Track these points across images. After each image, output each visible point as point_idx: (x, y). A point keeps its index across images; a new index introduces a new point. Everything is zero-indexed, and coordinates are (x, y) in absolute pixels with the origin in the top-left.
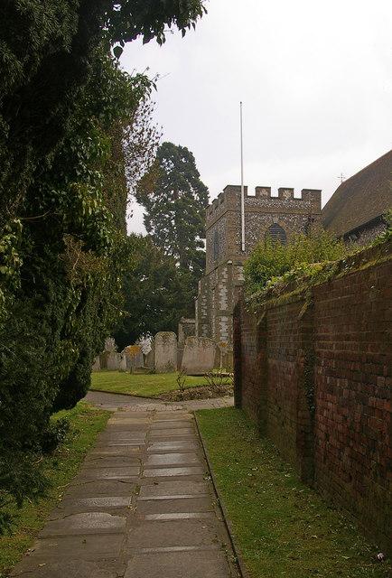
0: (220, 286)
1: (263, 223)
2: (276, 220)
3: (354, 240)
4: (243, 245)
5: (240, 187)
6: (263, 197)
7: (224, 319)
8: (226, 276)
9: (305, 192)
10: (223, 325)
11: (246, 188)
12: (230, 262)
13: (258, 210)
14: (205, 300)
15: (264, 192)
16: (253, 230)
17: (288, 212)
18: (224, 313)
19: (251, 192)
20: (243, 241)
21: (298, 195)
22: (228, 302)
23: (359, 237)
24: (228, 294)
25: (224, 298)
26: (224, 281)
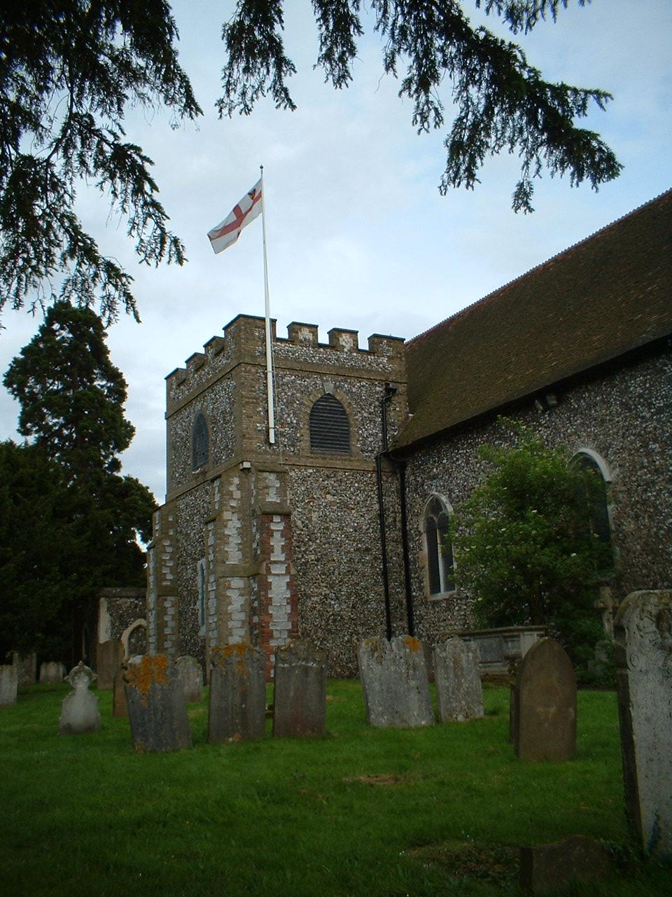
0: (227, 515)
1: (305, 391)
2: (329, 388)
3: (547, 408)
4: (272, 432)
5: (263, 320)
6: (304, 343)
7: (237, 583)
8: (237, 494)
9: (375, 339)
10: (233, 595)
11: (273, 322)
12: (247, 465)
13: (295, 366)
14: (169, 550)
15: (305, 334)
16: (289, 403)
17: (344, 373)
18: (234, 572)
19: (282, 333)
20: (272, 424)
21: (364, 345)
22: (243, 547)
23: (561, 401)
24: (243, 532)
25: (235, 540)
26: (233, 504)
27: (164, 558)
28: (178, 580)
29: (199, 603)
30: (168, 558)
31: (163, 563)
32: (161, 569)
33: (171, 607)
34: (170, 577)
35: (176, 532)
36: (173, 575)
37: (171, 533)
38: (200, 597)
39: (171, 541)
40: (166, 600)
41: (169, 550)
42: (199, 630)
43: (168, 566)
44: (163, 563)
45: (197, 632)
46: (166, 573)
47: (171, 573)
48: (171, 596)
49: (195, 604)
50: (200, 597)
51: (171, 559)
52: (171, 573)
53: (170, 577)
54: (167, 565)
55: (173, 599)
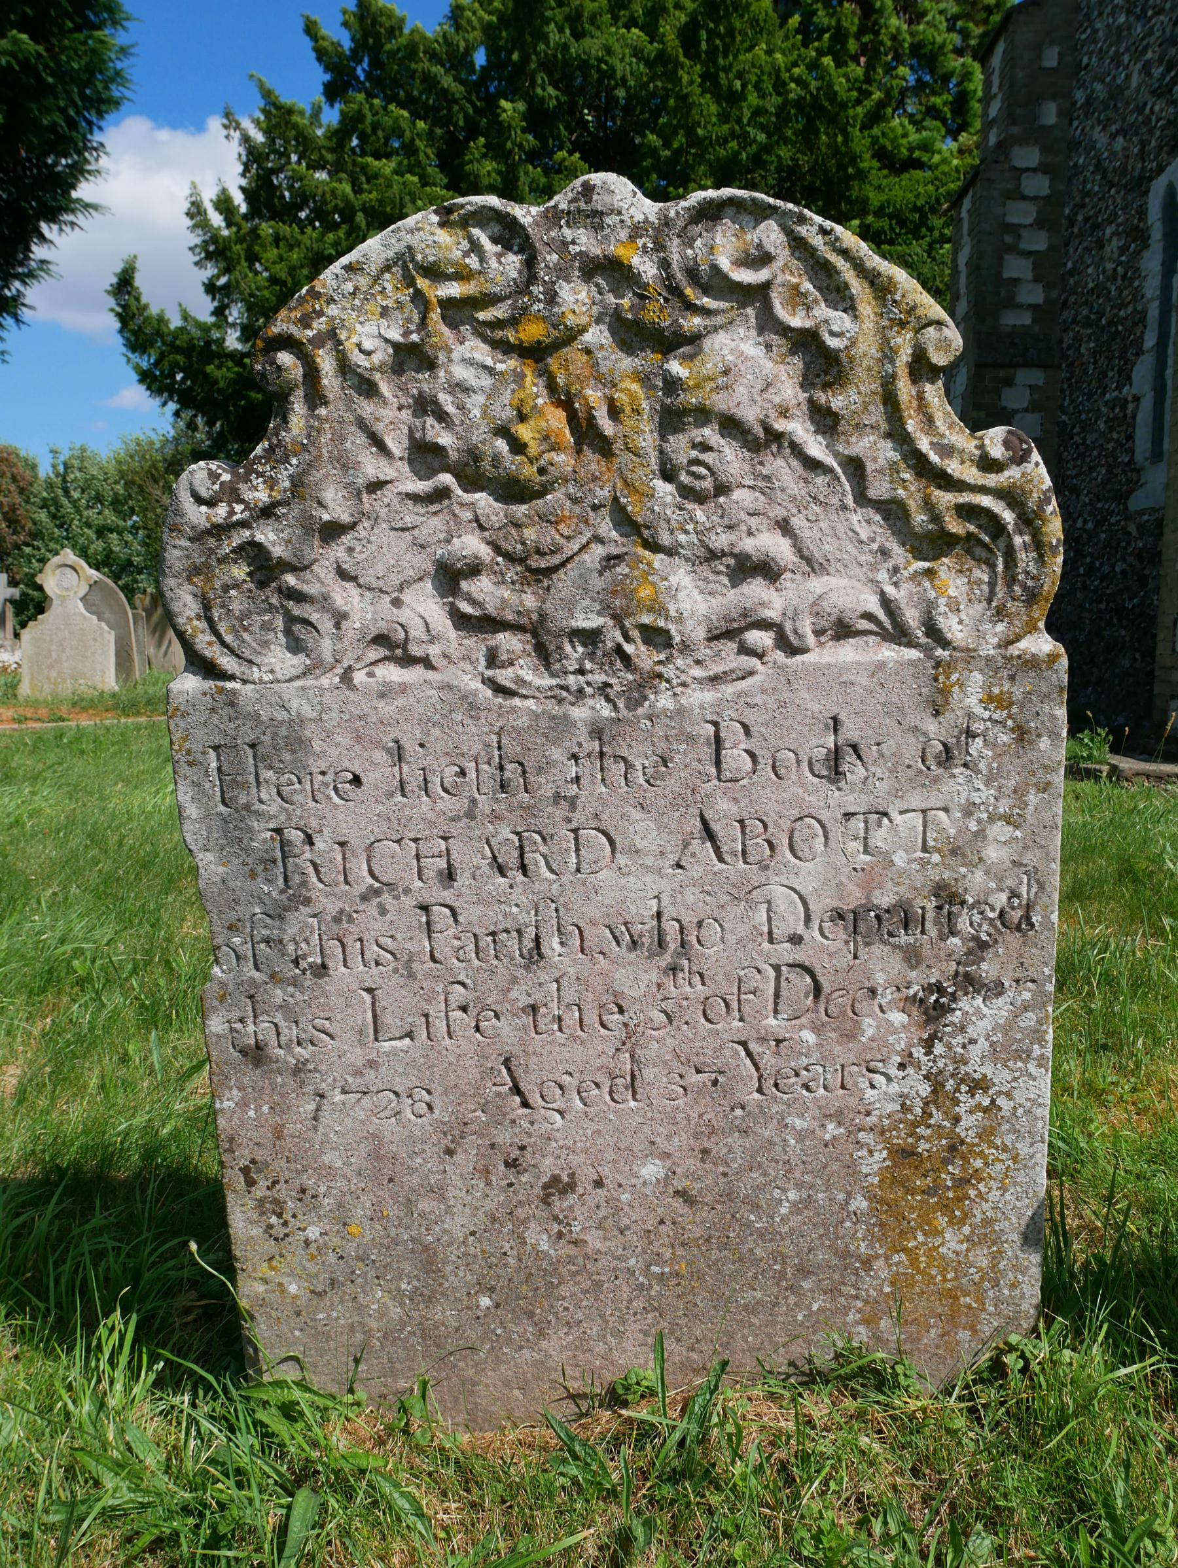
14: (1037, 185)
27: (1013, 219)
28: (1065, 304)
29: (1143, 370)
30: (1029, 220)
31: (1009, 239)
32: (1000, 260)
33: (1026, 410)
34: (1032, 294)
35: (1067, 115)
36: (1048, 287)
37: (1050, 114)
38: (1150, 340)
39: (1044, 150)
40: (1009, 382)
41: (1037, 185)
42: (1134, 485)
43: (1030, 253)
44: (1009, 239)
45: (1123, 497)
46: (1017, 281)
47: (1037, 279)
48: (1028, 365)
49: (1126, 377)
50: (1150, 340)
51: (1039, 224)
52: (1037, 279)
53: (1032, 294)
54: (1024, 246)
55: (1036, 377)
